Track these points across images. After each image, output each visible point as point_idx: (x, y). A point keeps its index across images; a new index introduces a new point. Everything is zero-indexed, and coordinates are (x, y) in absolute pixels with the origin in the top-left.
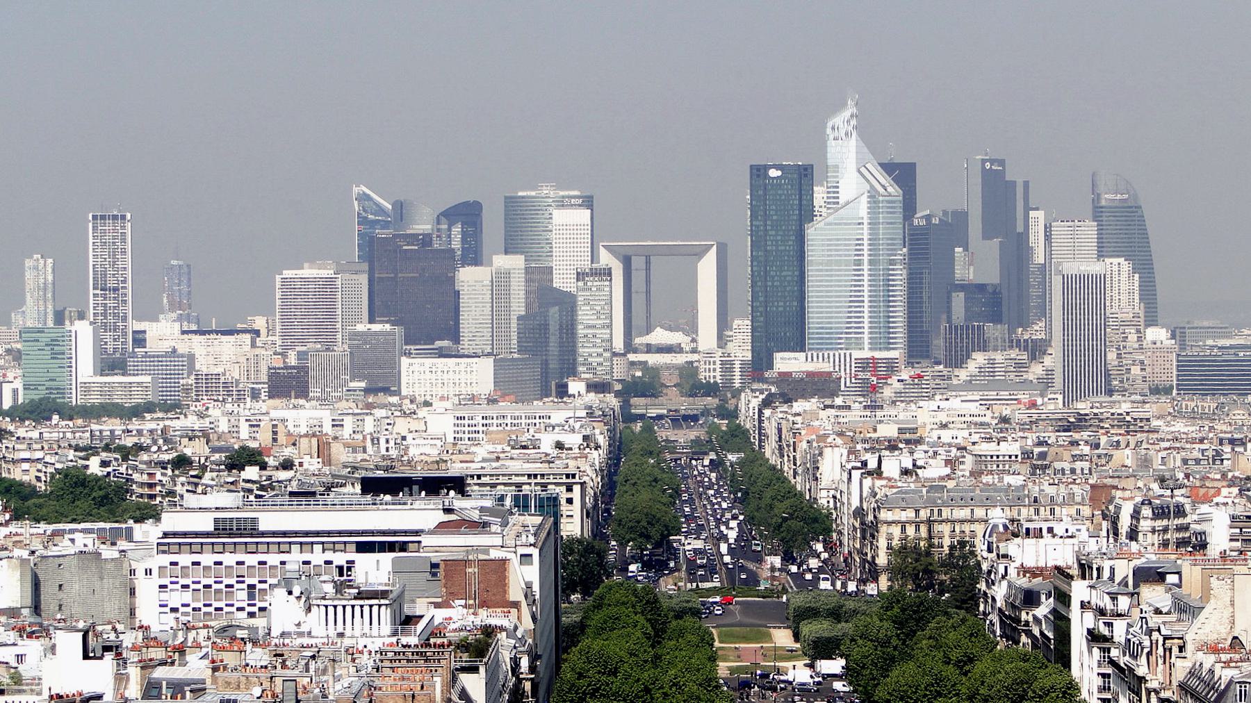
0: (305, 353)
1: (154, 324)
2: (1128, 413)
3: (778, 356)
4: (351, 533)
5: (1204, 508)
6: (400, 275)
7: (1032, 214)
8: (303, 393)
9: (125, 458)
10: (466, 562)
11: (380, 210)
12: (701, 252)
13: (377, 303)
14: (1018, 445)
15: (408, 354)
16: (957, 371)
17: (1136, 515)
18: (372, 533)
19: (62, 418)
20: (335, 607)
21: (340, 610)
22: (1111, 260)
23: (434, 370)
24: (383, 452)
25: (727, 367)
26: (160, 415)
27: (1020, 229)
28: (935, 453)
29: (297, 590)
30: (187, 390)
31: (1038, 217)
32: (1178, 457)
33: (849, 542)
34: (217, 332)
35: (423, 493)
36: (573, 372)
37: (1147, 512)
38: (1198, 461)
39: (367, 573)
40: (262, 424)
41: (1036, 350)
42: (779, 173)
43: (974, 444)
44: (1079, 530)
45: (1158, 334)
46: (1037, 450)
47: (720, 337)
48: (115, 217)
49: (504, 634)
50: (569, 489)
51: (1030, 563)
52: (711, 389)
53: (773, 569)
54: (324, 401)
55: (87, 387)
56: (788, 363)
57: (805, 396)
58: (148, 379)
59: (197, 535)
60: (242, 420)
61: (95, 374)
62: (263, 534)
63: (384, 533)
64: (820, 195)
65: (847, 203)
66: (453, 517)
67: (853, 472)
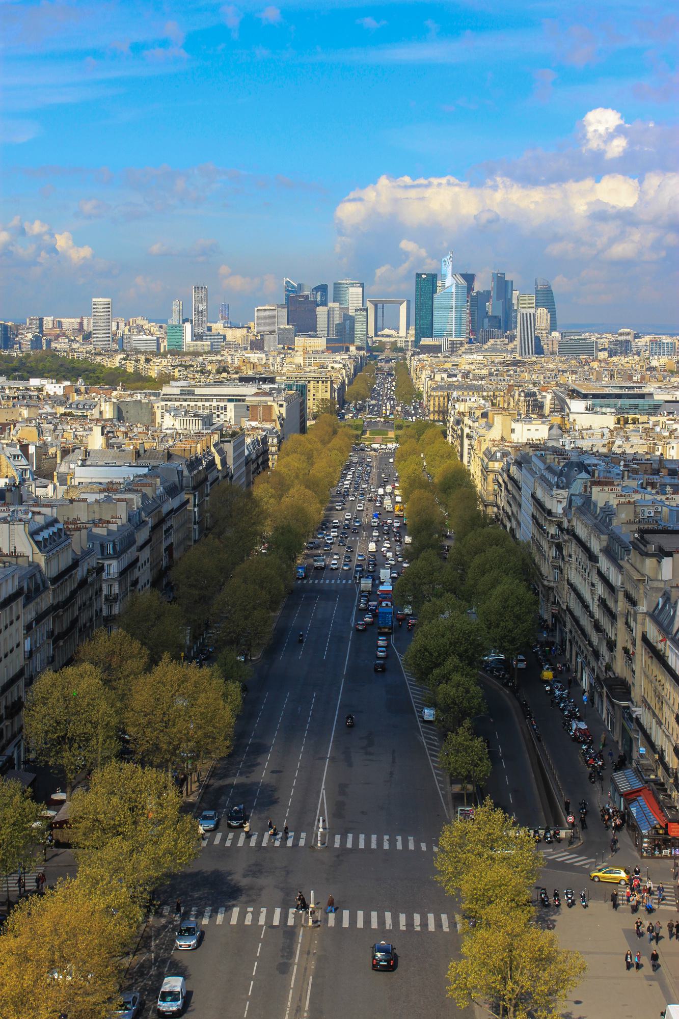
3: (423, 339)
4: (226, 395)
5: (544, 394)
9: (186, 370)
10: (258, 406)
11: (293, 286)
15: (299, 336)
17: (519, 395)
18: (233, 396)
25: (406, 343)
27: (509, 297)
29: (172, 414)
31: (516, 293)
33: (425, 402)
37: (522, 394)
38: (549, 378)
41: (512, 339)
45: (556, 334)
51: (462, 410)
52: (401, 350)
53: (397, 411)
56: (425, 341)
59: (174, 395)
62: (196, 395)
63: (237, 396)
64: (439, 283)
66: (261, 391)
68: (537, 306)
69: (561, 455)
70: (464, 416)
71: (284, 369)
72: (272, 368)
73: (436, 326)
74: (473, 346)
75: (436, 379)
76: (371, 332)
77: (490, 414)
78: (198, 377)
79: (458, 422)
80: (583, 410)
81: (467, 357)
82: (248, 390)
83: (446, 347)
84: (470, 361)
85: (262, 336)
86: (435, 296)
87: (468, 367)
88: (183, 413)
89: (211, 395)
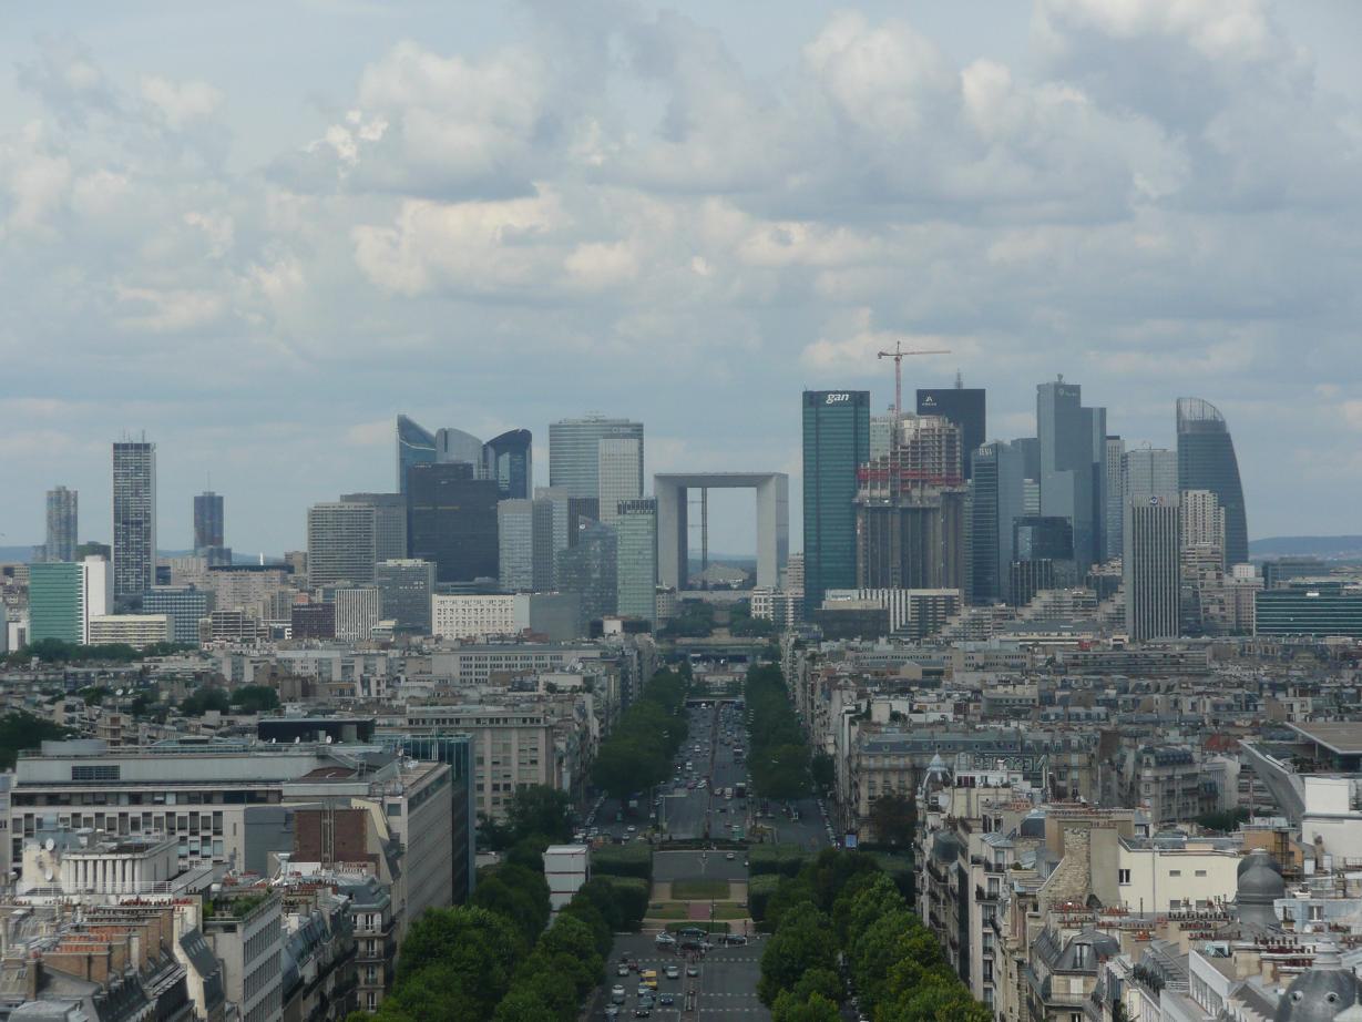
0: (333, 590)
2: (1182, 656)
3: (830, 593)
10: (321, 813)
14: (1035, 689)
15: (442, 592)
16: (1021, 610)
21: (90, 865)
22: (1196, 492)
23: (467, 608)
25: (780, 606)
28: (949, 696)
32: (1208, 701)
35: (298, 740)
36: (612, 612)
38: (1229, 707)
39: (235, 825)
41: (1108, 587)
43: (993, 687)
44: (1015, 780)
46: (1059, 694)
47: (779, 573)
49: (330, 889)
51: (959, 812)
52: (762, 627)
55: (97, 626)
56: (840, 599)
58: (163, 618)
60: (246, 661)
61: (107, 613)
62: (124, 784)
66: (328, 764)
69: (1282, 950)
70: (968, 830)
71: (401, 694)
72: (360, 693)
77: (1051, 827)
79: (949, 851)
80: (1344, 810)
81: (971, 646)
82: (288, 766)
85: (328, 593)
87: (973, 679)
88: (84, 841)
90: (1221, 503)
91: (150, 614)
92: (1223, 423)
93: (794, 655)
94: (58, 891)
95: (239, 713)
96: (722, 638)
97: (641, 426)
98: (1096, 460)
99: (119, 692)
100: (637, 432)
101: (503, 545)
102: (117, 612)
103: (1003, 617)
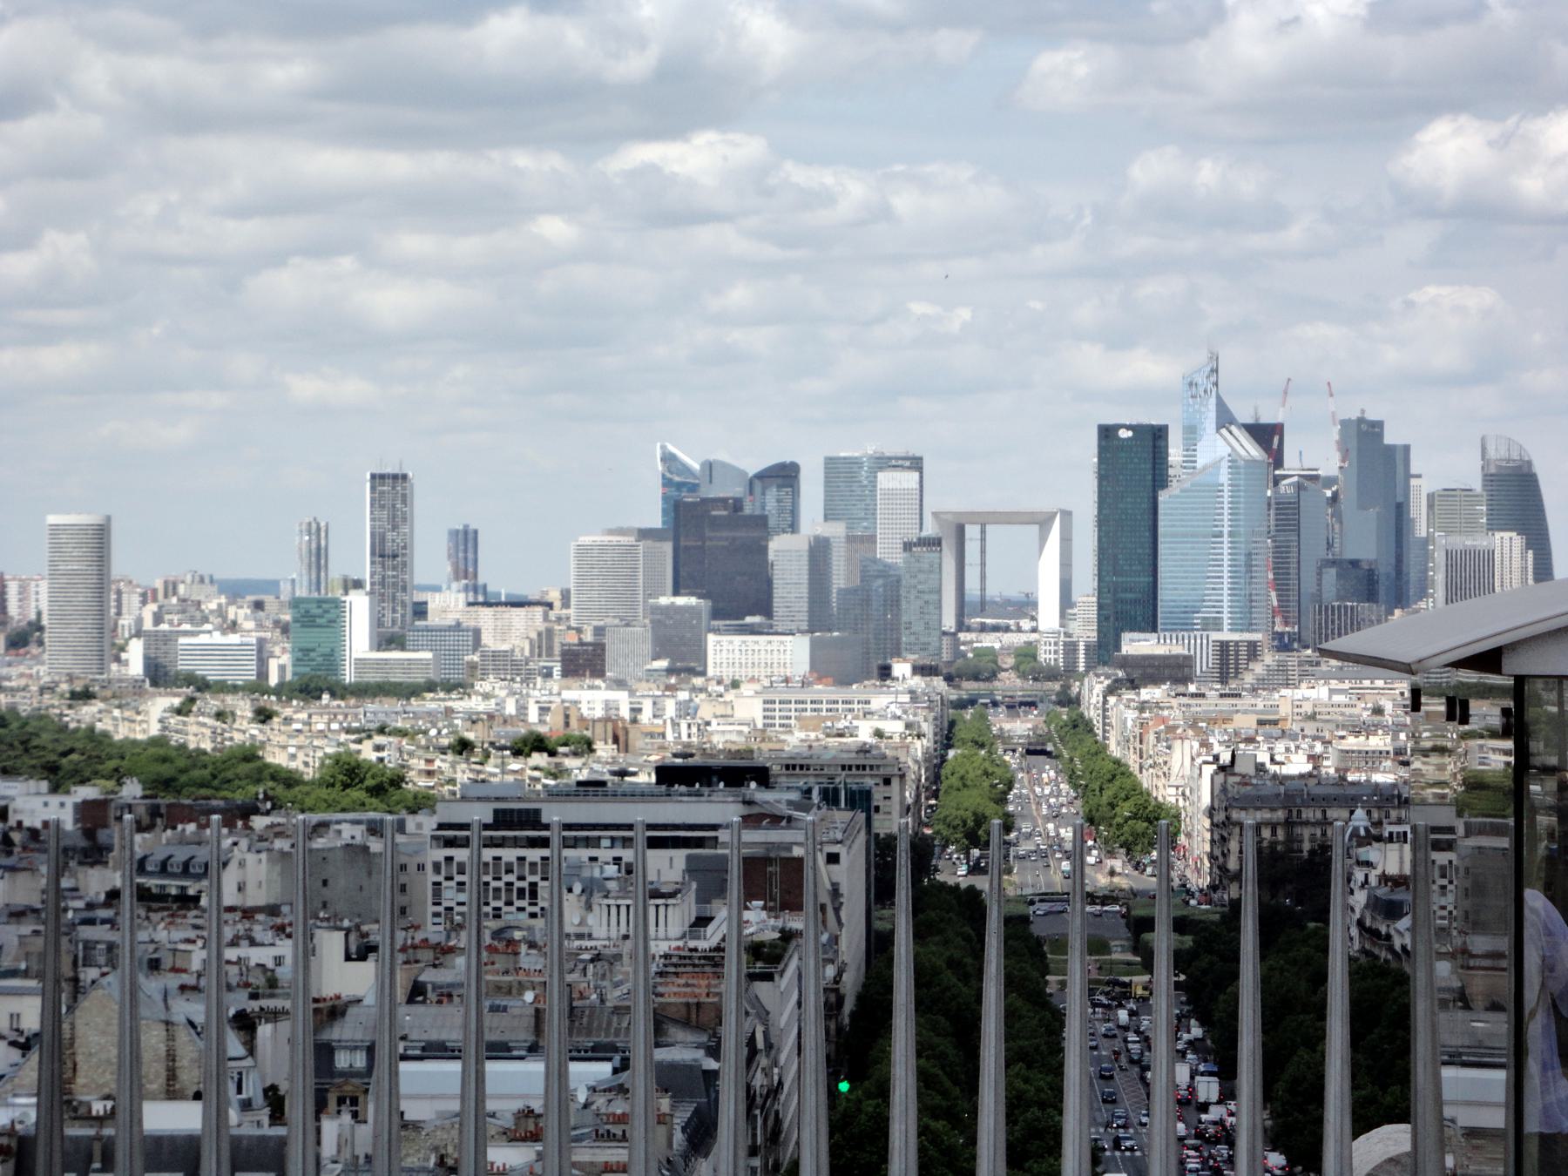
1: (437, 595)
3: (1126, 637)
6: (708, 543)
7: (1413, 482)
8: (599, 672)
10: (766, 861)
11: (686, 469)
12: (1043, 522)
13: (683, 573)
15: (717, 631)
18: (665, 827)
19: (333, 695)
20: (618, 906)
21: (623, 910)
22: (1502, 534)
23: (744, 648)
24: (685, 738)
25: (1071, 649)
26: (442, 695)
30: (473, 667)
34: (506, 604)
35: (722, 785)
36: (897, 653)
40: (553, 706)
42: (1130, 434)
43: (1343, 738)
47: (1063, 615)
48: (395, 477)
50: (887, 782)
52: (1051, 674)
54: (620, 684)
56: (1137, 645)
57: (1155, 680)
58: (428, 655)
61: (371, 649)
65: (1205, 468)
66: (755, 810)
67: (1205, 767)
68: (1493, 527)
73: (1169, 594)
74: (1292, 659)
75: (1237, 769)
76: (949, 622)
78: (445, 766)
83: (1205, 661)
84: (1307, 708)
85: (599, 631)
86: (1163, 496)
89: (594, 827)
90: (1528, 546)
91: (414, 651)
92: (1529, 463)
93: (1105, 702)
94: (590, 936)
95: (566, 755)
96: (1009, 683)
97: (921, 459)
98: (1400, 499)
99: (433, 732)
100: (916, 464)
101: (777, 583)
102: (378, 650)
103: (1310, 663)
